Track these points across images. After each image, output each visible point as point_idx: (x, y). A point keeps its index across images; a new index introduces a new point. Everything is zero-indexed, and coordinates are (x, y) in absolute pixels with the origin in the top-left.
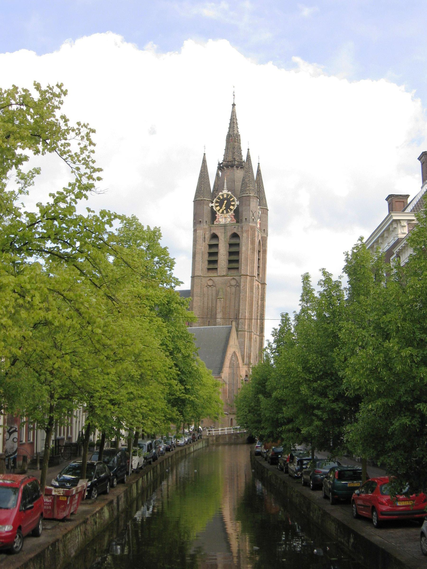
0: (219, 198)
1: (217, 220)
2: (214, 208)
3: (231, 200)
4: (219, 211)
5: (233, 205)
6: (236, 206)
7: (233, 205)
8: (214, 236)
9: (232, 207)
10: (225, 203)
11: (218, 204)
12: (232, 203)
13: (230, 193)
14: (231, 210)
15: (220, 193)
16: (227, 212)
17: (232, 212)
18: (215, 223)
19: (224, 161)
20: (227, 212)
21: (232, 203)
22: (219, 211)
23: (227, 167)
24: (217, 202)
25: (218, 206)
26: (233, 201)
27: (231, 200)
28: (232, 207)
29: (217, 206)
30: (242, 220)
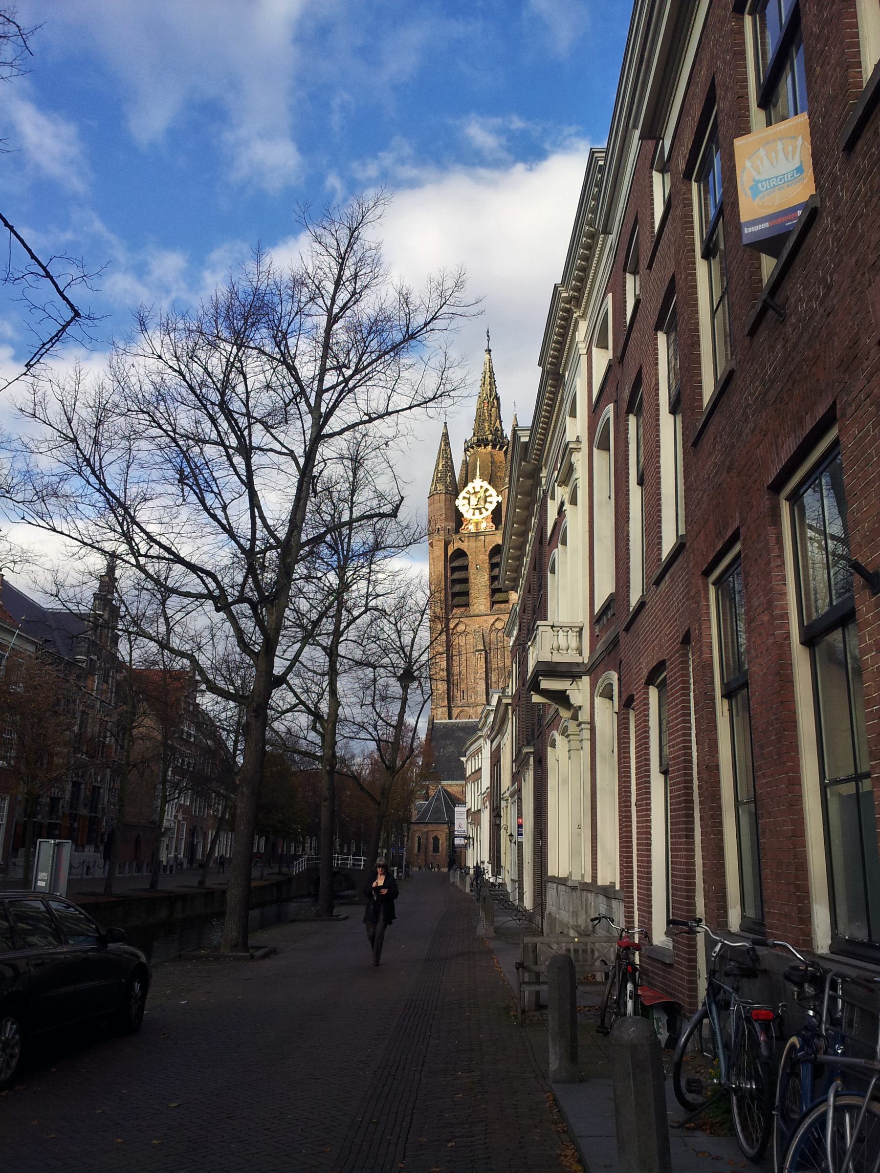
8: (460, 554)
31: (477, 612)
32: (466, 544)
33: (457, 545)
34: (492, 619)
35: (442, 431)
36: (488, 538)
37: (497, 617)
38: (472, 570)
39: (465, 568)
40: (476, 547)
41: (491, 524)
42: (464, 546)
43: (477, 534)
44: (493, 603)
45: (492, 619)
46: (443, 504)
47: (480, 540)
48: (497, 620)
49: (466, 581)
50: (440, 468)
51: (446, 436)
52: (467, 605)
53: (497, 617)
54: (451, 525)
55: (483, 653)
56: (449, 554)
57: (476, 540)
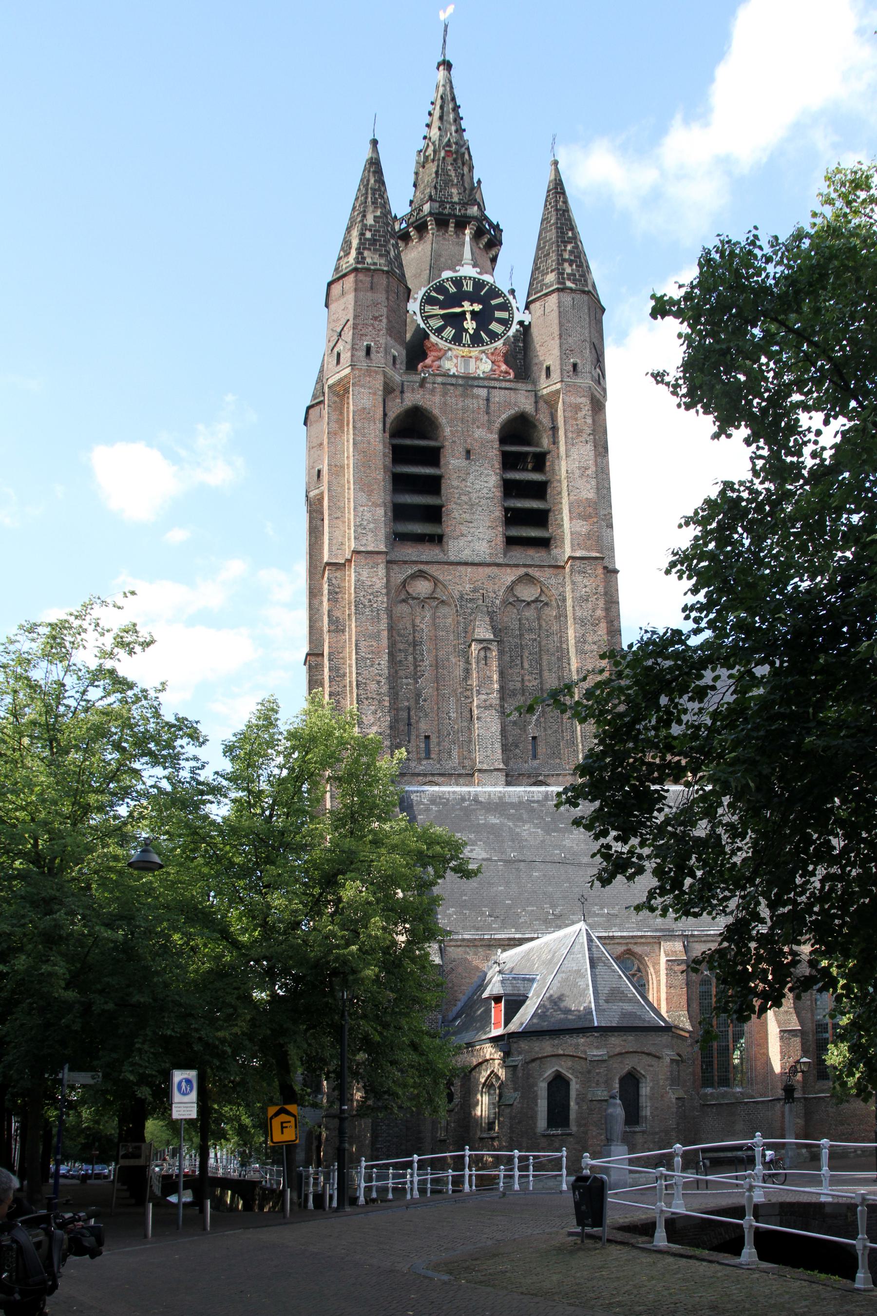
1: (428, 361)
3: (493, 302)
4: (439, 331)
6: (515, 327)
9: (495, 327)
12: (498, 314)
14: (494, 336)
21: (498, 314)
22: (439, 331)
27: (493, 302)
31: (466, 555)
32: (437, 399)
33: (412, 398)
34: (509, 576)
35: (366, 153)
36: (498, 396)
37: (522, 571)
39: (433, 456)
41: (504, 367)
42: (432, 402)
43: (468, 382)
44: (511, 542)
45: (509, 576)
47: (478, 397)
48: (520, 580)
49: (434, 485)
52: (438, 539)
53: (522, 571)
55: (494, 647)
56: (392, 415)
57: (464, 395)
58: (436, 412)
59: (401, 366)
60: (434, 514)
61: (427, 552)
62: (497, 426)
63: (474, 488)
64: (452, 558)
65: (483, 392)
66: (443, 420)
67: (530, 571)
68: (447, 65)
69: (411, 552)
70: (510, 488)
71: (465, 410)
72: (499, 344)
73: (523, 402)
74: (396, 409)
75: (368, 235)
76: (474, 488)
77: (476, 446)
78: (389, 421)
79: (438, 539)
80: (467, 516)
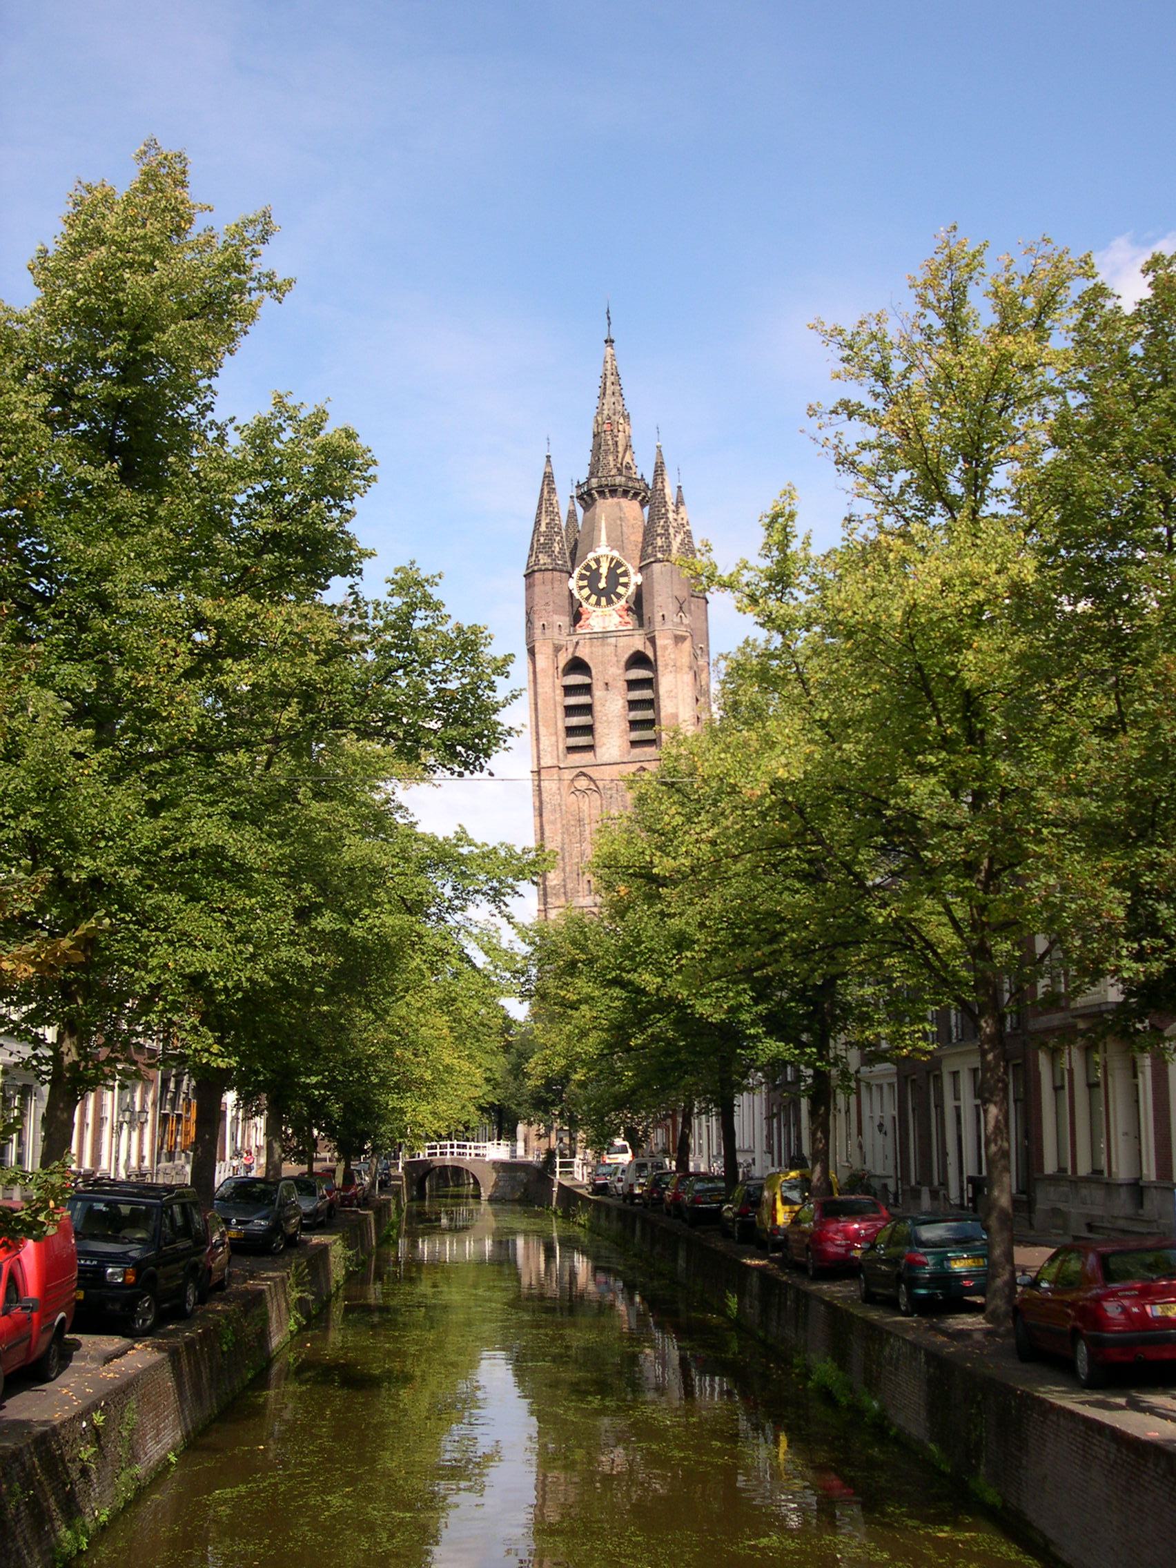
0: (588, 567)
1: (581, 623)
2: (575, 592)
3: (619, 571)
4: (587, 598)
5: (625, 585)
7: (625, 585)
8: (577, 665)
9: (620, 590)
10: (603, 580)
11: (585, 583)
12: (622, 580)
13: (616, 554)
14: (619, 596)
15: (591, 555)
16: (610, 602)
17: (623, 602)
18: (579, 631)
19: (592, 474)
20: (610, 602)
21: (622, 580)
22: (587, 598)
23: (601, 493)
24: (582, 577)
25: (584, 587)
26: (625, 574)
27: (619, 571)
28: (620, 590)
29: (581, 588)
30: (650, 621)
31: (605, 759)
36: (623, 641)
38: (598, 692)
39: (587, 689)
40: (603, 655)
42: (584, 653)
43: (604, 635)
46: (549, 587)
49: (587, 709)
50: (543, 528)
51: (548, 478)
54: (564, 620)
56: (561, 665)
57: (603, 645)
58: (587, 660)
59: (565, 631)
60: (588, 730)
61: (586, 758)
62: (623, 663)
63: (611, 708)
64: (599, 762)
65: (613, 640)
66: (591, 665)
67: (645, 765)
68: (609, 342)
69: (577, 758)
70: (633, 705)
71: (603, 655)
72: (623, 602)
73: (638, 643)
74: (563, 659)
75: (542, 540)
76: (611, 708)
77: (610, 681)
78: (560, 670)
79: (590, 748)
80: (606, 731)
